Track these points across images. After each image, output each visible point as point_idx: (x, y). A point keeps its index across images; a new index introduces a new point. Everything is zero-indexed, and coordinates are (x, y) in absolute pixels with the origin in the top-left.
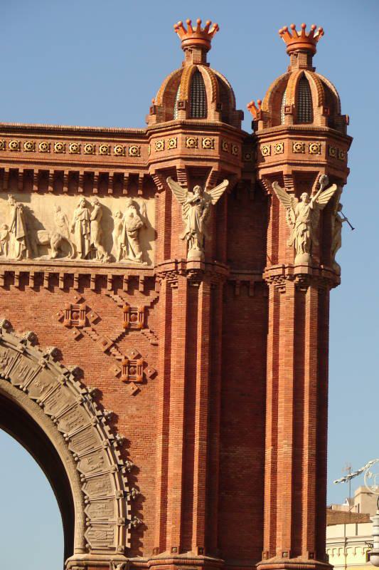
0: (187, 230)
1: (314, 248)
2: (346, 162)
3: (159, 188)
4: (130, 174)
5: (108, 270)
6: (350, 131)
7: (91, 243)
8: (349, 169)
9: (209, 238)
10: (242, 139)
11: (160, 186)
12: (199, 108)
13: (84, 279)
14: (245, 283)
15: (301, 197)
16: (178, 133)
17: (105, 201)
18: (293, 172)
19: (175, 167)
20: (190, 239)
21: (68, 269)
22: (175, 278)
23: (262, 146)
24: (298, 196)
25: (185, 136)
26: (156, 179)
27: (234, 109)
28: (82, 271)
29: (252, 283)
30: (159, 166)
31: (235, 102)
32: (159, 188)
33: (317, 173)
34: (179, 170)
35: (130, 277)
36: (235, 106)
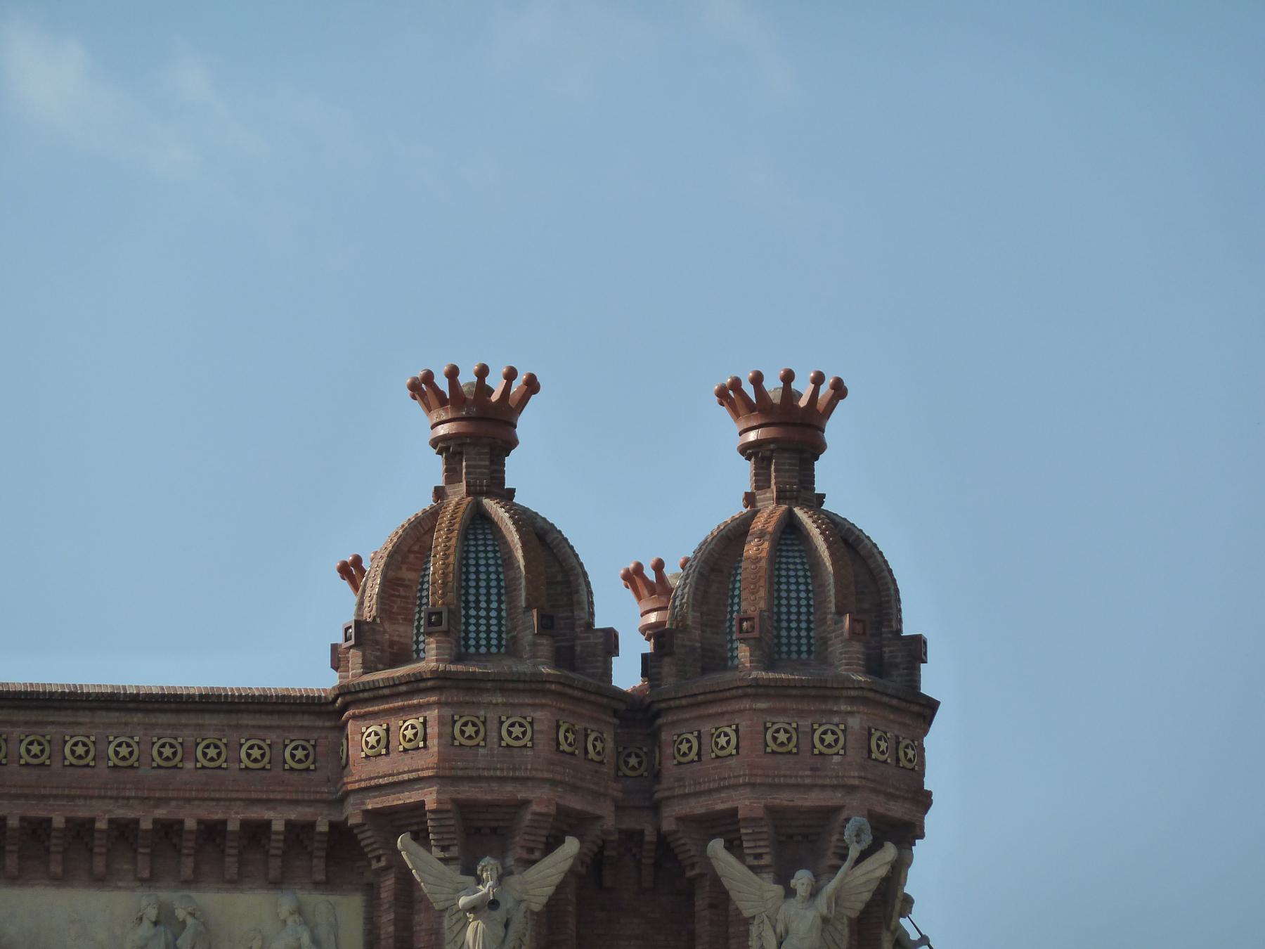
2: (917, 771)
3: (375, 865)
4: (289, 824)
6: (931, 681)
8: (929, 794)
10: (615, 713)
11: (379, 858)
12: (488, 625)
15: (793, 882)
16: (428, 706)
17: (212, 900)
18: (771, 811)
24: (783, 879)
25: (447, 712)
26: (367, 838)
27: (590, 625)
31: (591, 604)
32: (375, 865)
33: (837, 809)
34: (432, 811)
36: (592, 614)
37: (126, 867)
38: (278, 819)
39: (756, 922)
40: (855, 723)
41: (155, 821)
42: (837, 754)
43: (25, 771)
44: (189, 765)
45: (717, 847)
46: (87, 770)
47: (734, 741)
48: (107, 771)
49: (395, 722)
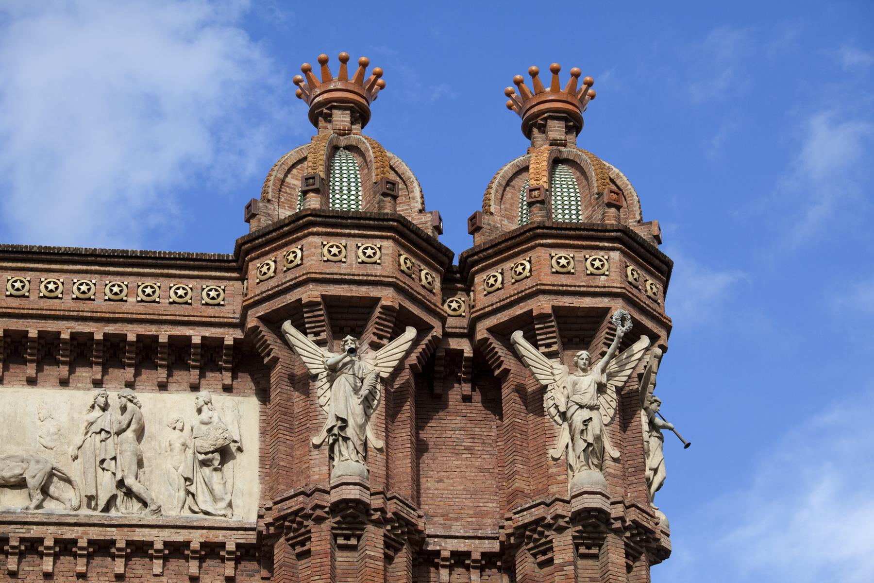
0: (331, 422)
1: (609, 463)
3: (266, 360)
5: (155, 531)
7: (119, 477)
9: (376, 442)
11: (269, 355)
13: (102, 548)
14: (460, 559)
19: (300, 300)
20: (336, 441)
21: (65, 529)
22: (303, 530)
23: (478, 279)
28: (95, 533)
29: (476, 556)
30: (262, 310)
33: (607, 310)
35: (203, 545)
37: (84, 374)
38: (196, 335)
39: (549, 388)
40: (616, 255)
41: (105, 335)
42: (604, 274)
43: (9, 299)
44: (132, 300)
45: (518, 336)
46: (57, 300)
47: (528, 266)
48: (71, 301)
49: (281, 254)
